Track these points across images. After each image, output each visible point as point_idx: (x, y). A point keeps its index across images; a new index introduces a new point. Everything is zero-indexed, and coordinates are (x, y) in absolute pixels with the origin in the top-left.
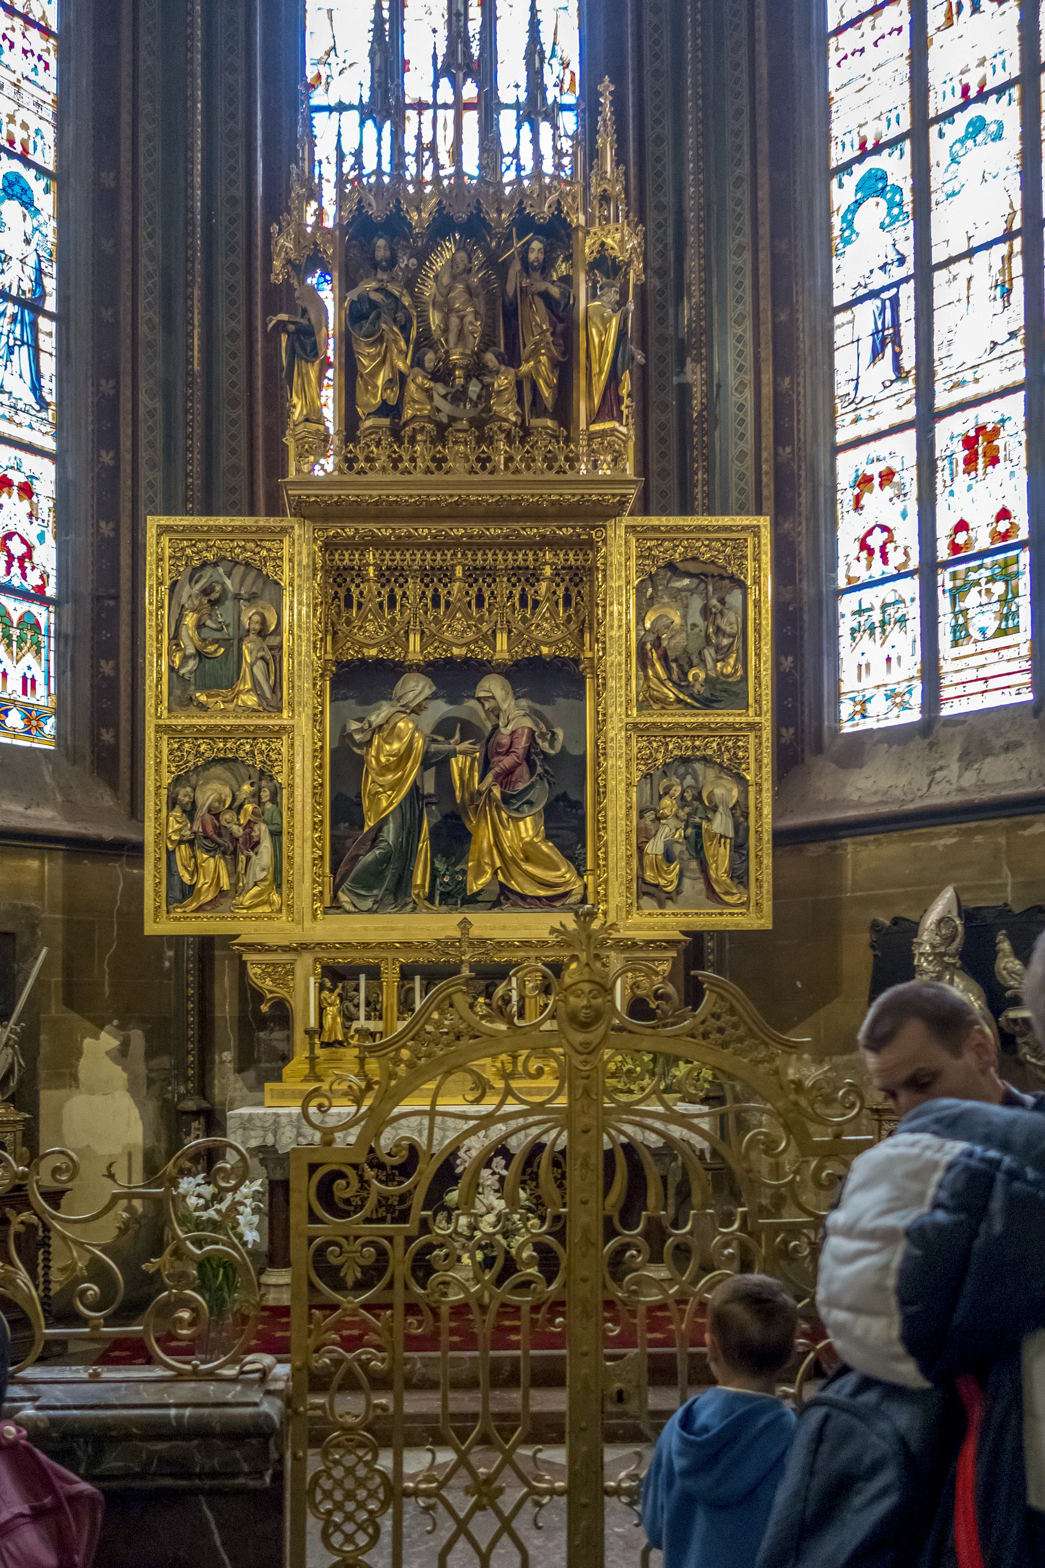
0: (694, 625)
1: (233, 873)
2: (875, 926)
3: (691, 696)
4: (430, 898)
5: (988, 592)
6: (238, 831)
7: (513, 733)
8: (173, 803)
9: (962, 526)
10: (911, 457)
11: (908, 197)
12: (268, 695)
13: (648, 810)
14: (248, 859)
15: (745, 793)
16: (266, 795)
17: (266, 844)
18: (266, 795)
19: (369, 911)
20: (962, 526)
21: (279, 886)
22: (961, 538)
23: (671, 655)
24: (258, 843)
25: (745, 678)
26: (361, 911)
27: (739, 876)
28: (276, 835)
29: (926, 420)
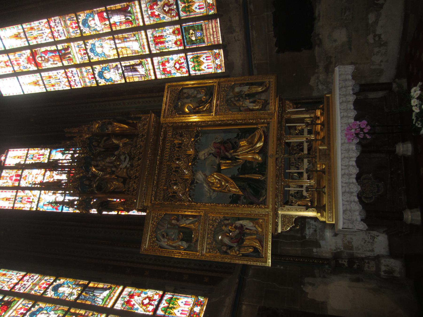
0: (191, 101)
1: (251, 234)
2: (278, 52)
3: (209, 99)
4: (263, 175)
5: (192, 34)
6: (237, 231)
7: (215, 148)
8: (226, 253)
9: (176, 43)
10: (159, 58)
11: (104, 65)
12: (196, 219)
13: (240, 109)
14: (247, 229)
15: (237, 84)
16: (226, 222)
17: (241, 222)
18: (226, 222)
19: (266, 191)
20: (176, 43)
21: (256, 219)
22: (179, 43)
23: (198, 105)
24: (241, 225)
25: (206, 87)
26: (266, 194)
27: (261, 84)
28: (239, 219)
29: (151, 55)
